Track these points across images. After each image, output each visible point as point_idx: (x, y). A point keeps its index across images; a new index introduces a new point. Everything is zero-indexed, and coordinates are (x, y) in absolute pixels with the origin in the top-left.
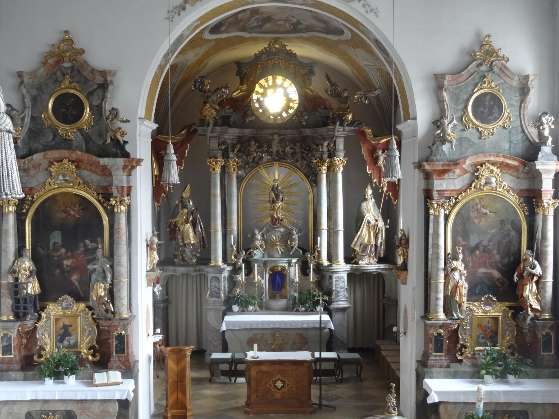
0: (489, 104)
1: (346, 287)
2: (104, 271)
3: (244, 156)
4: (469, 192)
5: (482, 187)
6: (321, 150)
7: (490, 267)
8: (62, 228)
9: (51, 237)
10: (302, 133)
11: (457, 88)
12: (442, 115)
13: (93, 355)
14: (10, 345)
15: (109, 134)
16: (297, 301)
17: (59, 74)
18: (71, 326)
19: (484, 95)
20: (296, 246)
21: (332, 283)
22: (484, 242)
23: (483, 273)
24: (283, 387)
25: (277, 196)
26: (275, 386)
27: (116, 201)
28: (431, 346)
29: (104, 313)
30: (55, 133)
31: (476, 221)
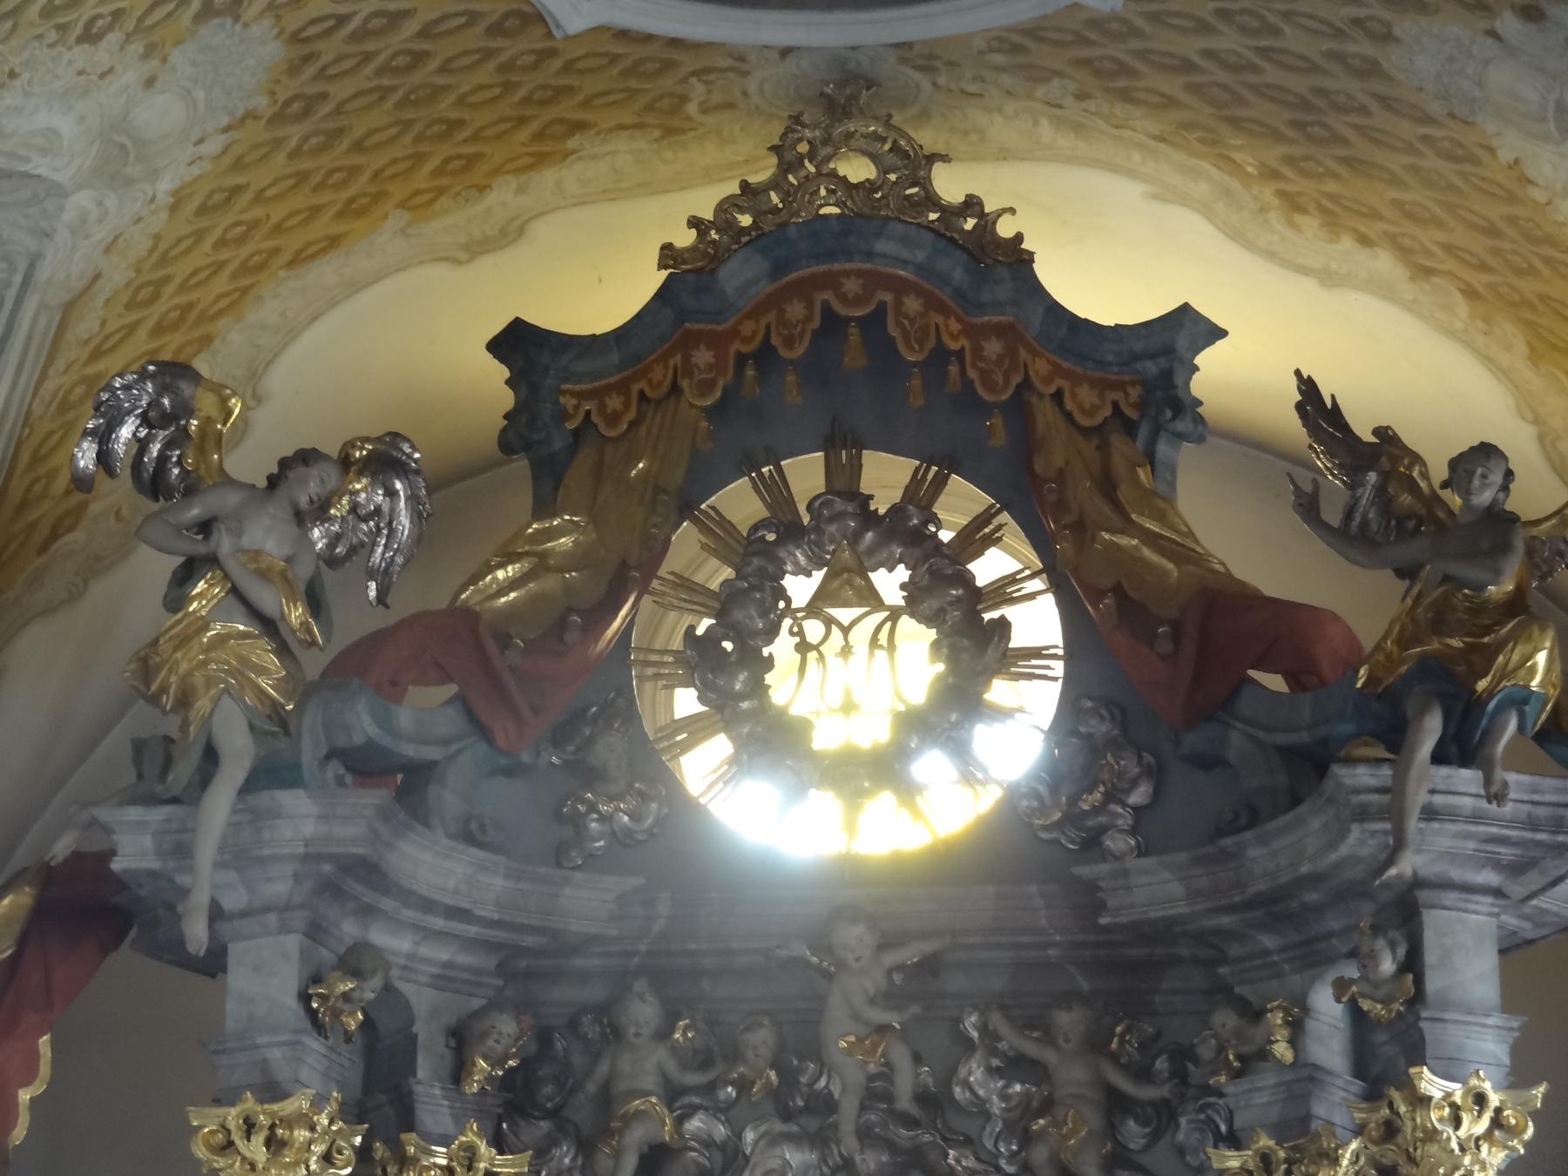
6: (1282, 1050)
10: (1101, 907)
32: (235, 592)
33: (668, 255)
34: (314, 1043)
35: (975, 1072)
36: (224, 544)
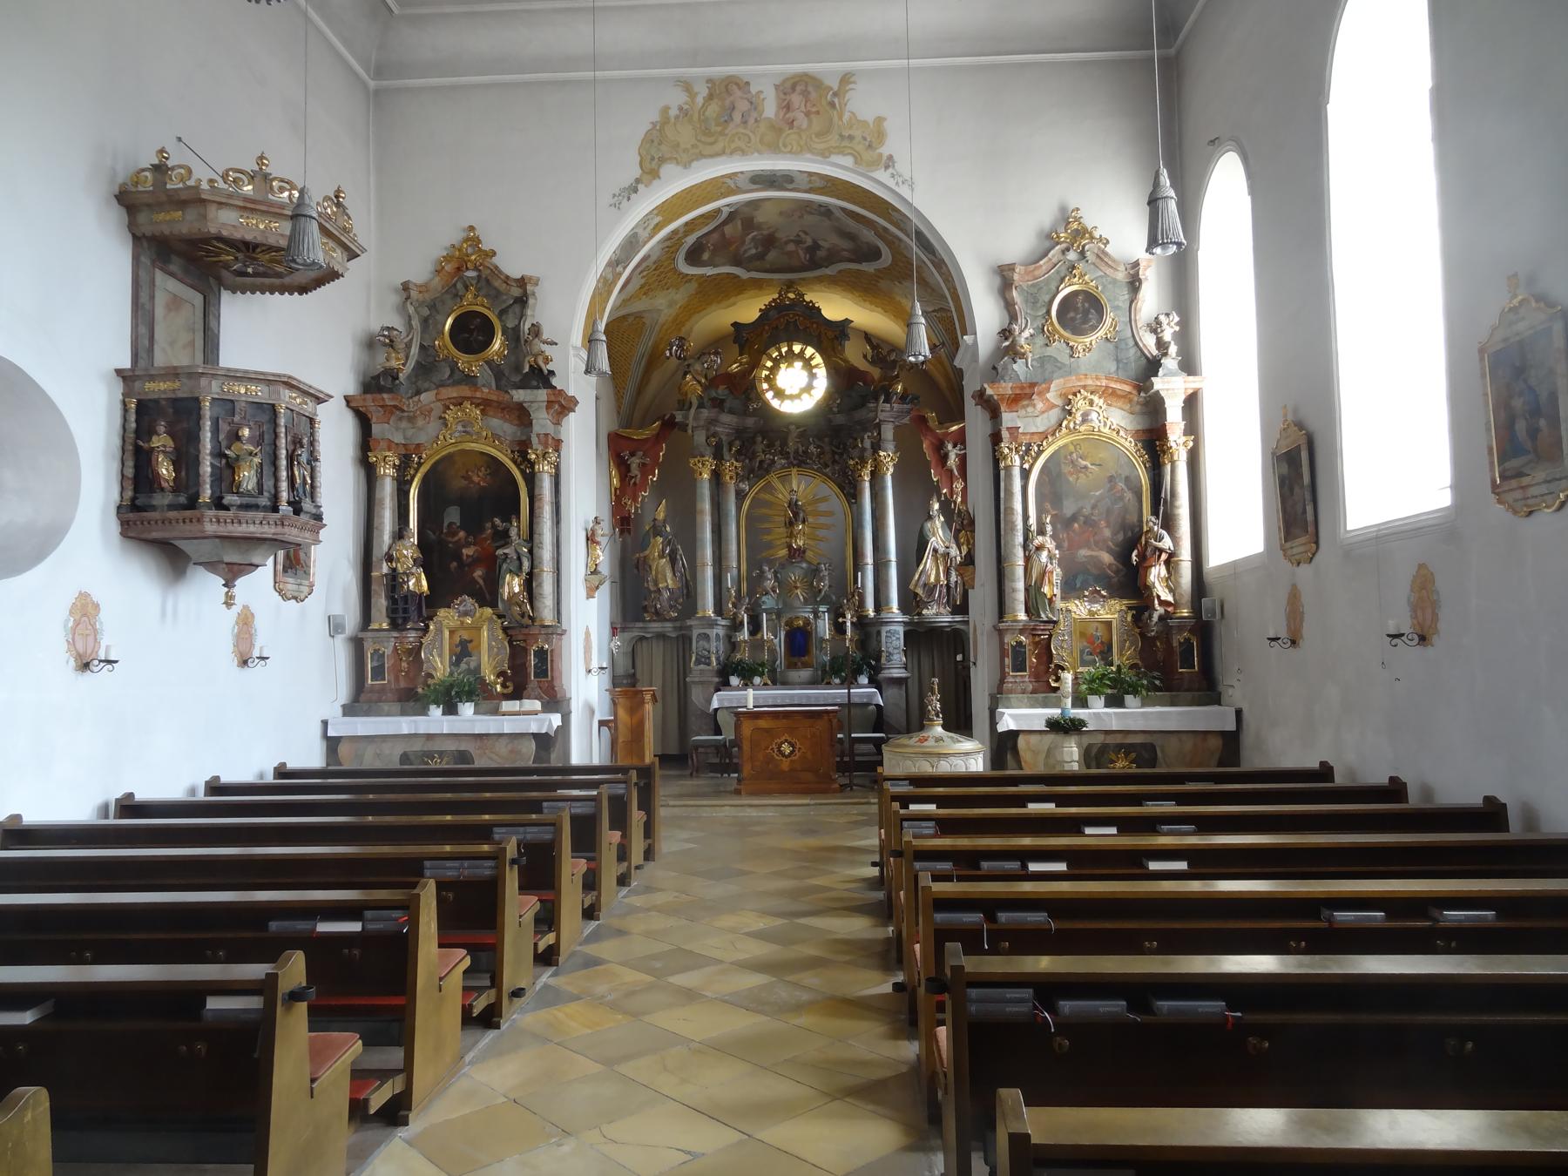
0: (1083, 306)
1: (902, 647)
2: (519, 559)
3: (747, 461)
4: (1057, 435)
5: (1077, 427)
7: (1097, 547)
8: (462, 501)
9: (445, 514)
11: (1033, 285)
12: (1013, 317)
13: (504, 686)
14: (383, 665)
15: (527, 359)
16: (827, 669)
17: (459, 286)
18: (471, 641)
19: (1075, 294)
20: (826, 588)
21: (880, 642)
22: (1085, 510)
23: (1086, 557)
24: (792, 752)
25: (796, 514)
26: (780, 751)
27: (536, 455)
28: (1008, 661)
29: (519, 618)
30: (454, 367)
31: (1071, 479)
32: (693, 377)
33: (761, 310)
34: (708, 448)
35: (812, 447)
36: (691, 369)
